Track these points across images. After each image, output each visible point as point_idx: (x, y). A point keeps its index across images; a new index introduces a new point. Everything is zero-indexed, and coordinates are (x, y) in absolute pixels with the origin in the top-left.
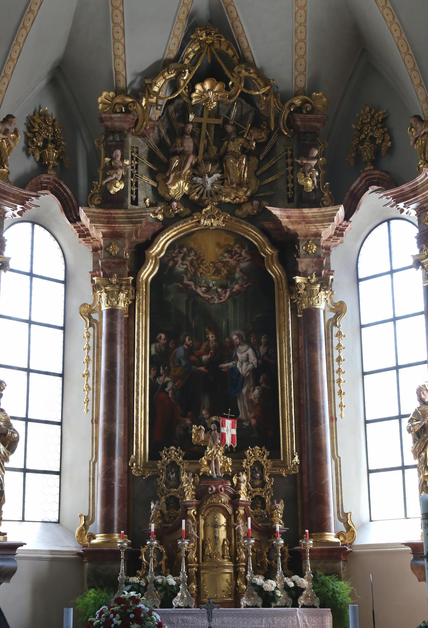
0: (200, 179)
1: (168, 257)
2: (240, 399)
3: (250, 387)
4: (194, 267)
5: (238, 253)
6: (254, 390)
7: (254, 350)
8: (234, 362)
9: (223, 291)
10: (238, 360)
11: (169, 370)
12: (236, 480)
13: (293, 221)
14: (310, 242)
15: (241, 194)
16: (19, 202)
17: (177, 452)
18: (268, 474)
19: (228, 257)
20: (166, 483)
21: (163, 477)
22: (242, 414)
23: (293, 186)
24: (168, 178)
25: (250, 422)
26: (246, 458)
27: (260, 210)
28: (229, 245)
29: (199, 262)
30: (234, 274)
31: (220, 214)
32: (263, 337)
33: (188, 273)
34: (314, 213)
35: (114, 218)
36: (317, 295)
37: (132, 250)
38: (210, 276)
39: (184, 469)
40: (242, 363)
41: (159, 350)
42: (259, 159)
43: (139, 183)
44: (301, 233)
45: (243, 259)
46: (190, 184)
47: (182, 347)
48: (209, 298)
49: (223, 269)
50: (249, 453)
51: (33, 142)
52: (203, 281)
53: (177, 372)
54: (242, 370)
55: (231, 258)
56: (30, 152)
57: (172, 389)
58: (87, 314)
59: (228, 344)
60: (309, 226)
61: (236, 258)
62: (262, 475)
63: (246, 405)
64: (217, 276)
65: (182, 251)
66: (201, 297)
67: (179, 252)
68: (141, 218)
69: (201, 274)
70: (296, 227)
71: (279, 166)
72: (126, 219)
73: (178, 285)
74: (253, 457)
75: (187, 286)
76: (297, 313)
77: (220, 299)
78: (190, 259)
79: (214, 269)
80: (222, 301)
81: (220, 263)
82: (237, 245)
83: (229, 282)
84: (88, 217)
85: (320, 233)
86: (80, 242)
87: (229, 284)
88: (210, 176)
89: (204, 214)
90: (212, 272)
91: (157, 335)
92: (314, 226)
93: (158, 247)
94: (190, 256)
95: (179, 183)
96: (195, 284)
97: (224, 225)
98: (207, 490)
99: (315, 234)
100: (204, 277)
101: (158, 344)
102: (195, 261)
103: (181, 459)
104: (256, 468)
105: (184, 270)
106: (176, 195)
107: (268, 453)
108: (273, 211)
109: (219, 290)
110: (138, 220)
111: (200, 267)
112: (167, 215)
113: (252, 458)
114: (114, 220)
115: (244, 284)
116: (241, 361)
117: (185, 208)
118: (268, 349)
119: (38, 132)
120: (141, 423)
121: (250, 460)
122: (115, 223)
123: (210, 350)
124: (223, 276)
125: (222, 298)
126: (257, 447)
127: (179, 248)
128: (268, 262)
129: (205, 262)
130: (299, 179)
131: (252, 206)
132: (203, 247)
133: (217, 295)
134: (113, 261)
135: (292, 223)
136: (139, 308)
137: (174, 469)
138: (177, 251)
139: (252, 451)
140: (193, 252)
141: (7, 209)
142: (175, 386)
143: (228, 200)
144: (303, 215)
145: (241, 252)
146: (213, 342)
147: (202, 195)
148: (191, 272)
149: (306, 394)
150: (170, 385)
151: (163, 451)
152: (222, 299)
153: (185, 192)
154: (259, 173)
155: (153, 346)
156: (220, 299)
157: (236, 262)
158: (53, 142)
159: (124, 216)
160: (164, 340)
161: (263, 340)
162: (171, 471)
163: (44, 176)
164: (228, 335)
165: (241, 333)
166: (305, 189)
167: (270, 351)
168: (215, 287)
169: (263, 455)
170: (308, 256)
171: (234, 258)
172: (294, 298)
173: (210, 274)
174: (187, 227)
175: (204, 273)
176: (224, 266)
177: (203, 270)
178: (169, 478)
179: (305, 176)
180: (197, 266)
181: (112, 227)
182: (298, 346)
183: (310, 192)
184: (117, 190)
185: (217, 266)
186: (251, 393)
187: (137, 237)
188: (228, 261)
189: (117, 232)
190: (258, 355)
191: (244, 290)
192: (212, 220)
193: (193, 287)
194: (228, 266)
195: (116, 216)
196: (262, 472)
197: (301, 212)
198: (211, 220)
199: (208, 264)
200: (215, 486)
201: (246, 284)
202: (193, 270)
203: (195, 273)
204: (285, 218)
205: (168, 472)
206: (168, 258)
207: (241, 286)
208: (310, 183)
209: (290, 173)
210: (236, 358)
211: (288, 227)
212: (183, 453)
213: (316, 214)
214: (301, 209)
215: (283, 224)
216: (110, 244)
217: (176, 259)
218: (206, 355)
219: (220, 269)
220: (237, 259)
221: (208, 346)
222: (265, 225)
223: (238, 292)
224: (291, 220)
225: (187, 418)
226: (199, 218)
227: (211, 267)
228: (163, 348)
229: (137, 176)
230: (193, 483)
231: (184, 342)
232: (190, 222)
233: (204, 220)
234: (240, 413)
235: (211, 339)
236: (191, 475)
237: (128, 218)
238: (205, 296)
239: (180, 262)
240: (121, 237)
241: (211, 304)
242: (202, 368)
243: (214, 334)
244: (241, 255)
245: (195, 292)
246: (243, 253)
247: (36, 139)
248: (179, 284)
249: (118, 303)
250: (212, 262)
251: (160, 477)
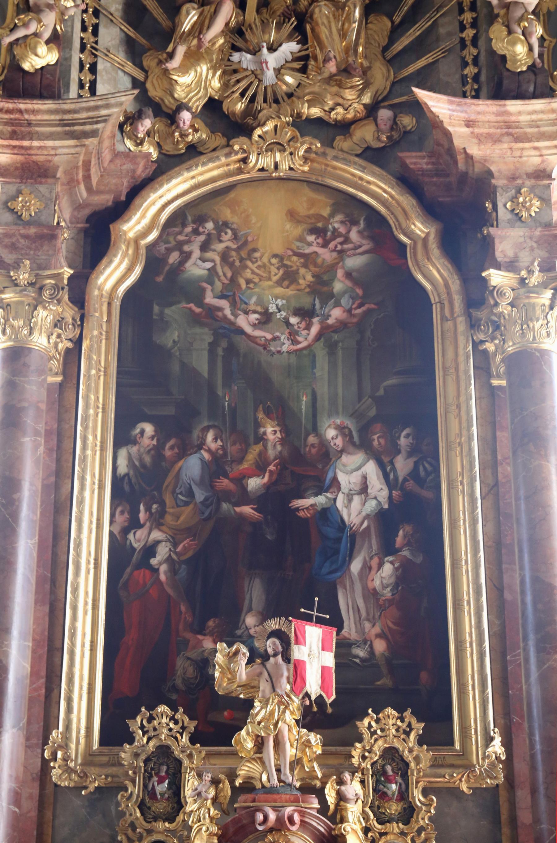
0: (249, 56)
1: (167, 242)
2: (345, 588)
3: (371, 558)
4: (231, 265)
5: (340, 235)
6: (380, 565)
7: (381, 465)
8: (328, 495)
9: (303, 323)
10: (339, 489)
11: (162, 513)
12: (333, 794)
13: (481, 135)
14: (523, 190)
15: (350, 97)
17: (176, 723)
18: (421, 785)
19: (315, 244)
20: (142, 806)
21: (135, 790)
22: (349, 625)
23: (476, 71)
24: (171, 56)
25: (371, 646)
26: (361, 740)
27: (396, 135)
28: (319, 217)
29: (244, 254)
30: (329, 283)
31: (297, 142)
32: (404, 433)
33: (216, 280)
34: (535, 112)
35: (29, 124)
36: (546, 317)
37: (80, 225)
38: (271, 287)
39: (192, 769)
40: (350, 498)
41: (137, 463)
42: (393, 22)
43: (100, 67)
44: (499, 171)
45: (352, 249)
46: (224, 73)
47: (197, 455)
48: (266, 340)
49: (302, 271)
50: (370, 725)
52: (254, 299)
53: (182, 518)
54: (349, 515)
55: (325, 245)
57: (169, 560)
59: (314, 451)
60: (522, 149)
61: (336, 247)
62: (403, 786)
63: (361, 603)
64: (287, 287)
65: (201, 230)
66: (248, 336)
67: (196, 232)
68: (97, 123)
69: (248, 282)
70: (488, 152)
71: (442, 31)
72: (58, 125)
73: (190, 309)
74: (381, 737)
75: (212, 311)
76: (489, 375)
77: (295, 342)
78: (220, 247)
79: (281, 272)
80: (300, 346)
81: (295, 258)
82: (339, 217)
83: (317, 302)
85: (548, 169)
87: (318, 306)
88: (272, 49)
89: (257, 142)
90: (275, 279)
91: (134, 426)
92: (536, 148)
93: (143, 216)
94: (221, 241)
95: (199, 69)
96: (234, 305)
97: (306, 168)
98: (253, 821)
99: (536, 171)
100: (257, 290)
101: (134, 450)
102: (234, 253)
103: (185, 740)
104: (389, 769)
105: (206, 272)
106: (190, 99)
107: (419, 727)
108: (430, 103)
109: (293, 320)
110: (88, 128)
111: (246, 267)
112: (168, 148)
113: (376, 740)
114: (28, 129)
115: (354, 306)
116: (346, 491)
117: (213, 132)
118: (416, 464)
120: (83, 645)
121: (372, 746)
122: (31, 136)
123: (269, 464)
124: (303, 287)
125: (300, 339)
126: (389, 711)
127: (194, 222)
128: (415, 254)
129: (257, 255)
130: (494, 41)
131: (377, 125)
132: (254, 220)
133: (287, 331)
134: (22, 231)
135: (480, 139)
136: (89, 358)
137: (165, 768)
138: (189, 229)
139: (378, 721)
140: (229, 231)
142: (176, 553)
143: (316, 112)
144: (506, 118)
145: (349, 231)
146: (275, 446)
147: (253, 99)
148: (223, 278)
149: (522, 568)
150: (163, 551)
151: (139, 719)
152: (299, 343)
153: (213, 93)
154: (389, 55)
155: (123, 453)
156: (295, 342)
157: (335, 254)
159: (53, 117)
160: (152, 438)
161: (403, 441)
162: (157, 774)
164: (315, 429)
165: (350, 423)
166: (509, 65)
167: (421, 468)
168: (284, 314)
169: (408, 734)
170: (518, 224)
171: (332, 245)
172: (482, 337)
173: (270, 283)
174: (215, 173)
175: (256, 280)
176: (305, 266)
177: (253, 272)
178: (152, 795)
179: (510, 32)
180: (237, 263)
181: (22, 147)
182: (494, 452)
183: (521, 72)
184: (39, 63)
185: (289, 263)
186: (373, 572)
187: (89, 189)
188: (316, 253)
189: (36, 163)
190: (392, 476)
191: (355, 320)
192: (278, 155)
193: (228, 312)
194: (316, 265)
195: (32, 117)
196: (405, 776)
197: (503, 109)
198: (275, 157)
199: (265, 260)
200: (275, 809)
201: (360, 306)
202: (229, 274)
203: (233, 280)
204: (460, 125)
205: (150, 777)
206: (166, 246)
207: (349, 311)
208: (520, 49)
209: (468, 43)
210: (335, 484)
211: (469, 151)
212: (192, 725)
213: (541, 116)
214: (502, 102)
215: (458, 143)
216: (19, 192)
217: (186, 248)
218: (258, 476)
219: (297, 272)
220: (339, 248)
221: (262, 455)
222: (408, 161)
223: (342, 325)
224: (477, 130)
225: (205, 635)
226: (244, 151)
227: (272, 267)
228: (148, 459)
229: (96, 50)
230: (215, 800)
231: (201, 446)
232: (223, 160)
233: (259, 154)
234: (346, 624)
235: (270, 437)
236: (208, 777)
237: (63, 123)
238: (258, 333)
239: (197, 253)
240: (46, 176)
241: (273, 354)
242: (247, 510)
243: (278, 425)
244: (347, 240)
245: (233, 324)
246: (354, 235)
248: (192, 305)
249: (31, 333)
250: (275, 256)
251: (126, 790)
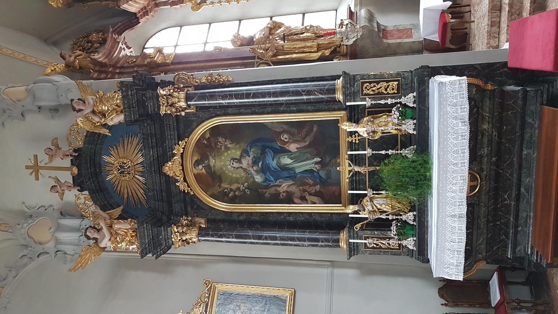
51: (89, 49)
56: (95, 50)
58: (198, 6)
84: (128, 2)
86: (153, 16)
119: (83, 46)
247: (87, 47)
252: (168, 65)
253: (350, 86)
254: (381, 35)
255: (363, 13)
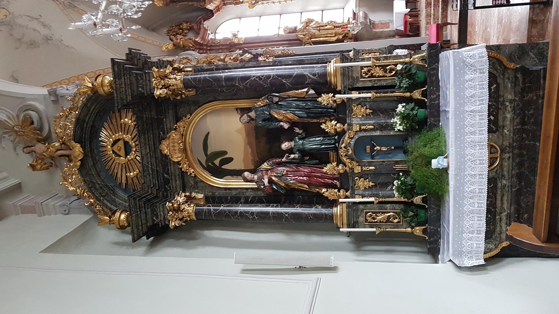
16: (206, 32)
84: (210, 4)
141: (210, 38)
158: (179, 26)
163: (194, 27)
252: (241, 44)
253: (357, 55)
254: (372, 27)
255: (361, 14)
